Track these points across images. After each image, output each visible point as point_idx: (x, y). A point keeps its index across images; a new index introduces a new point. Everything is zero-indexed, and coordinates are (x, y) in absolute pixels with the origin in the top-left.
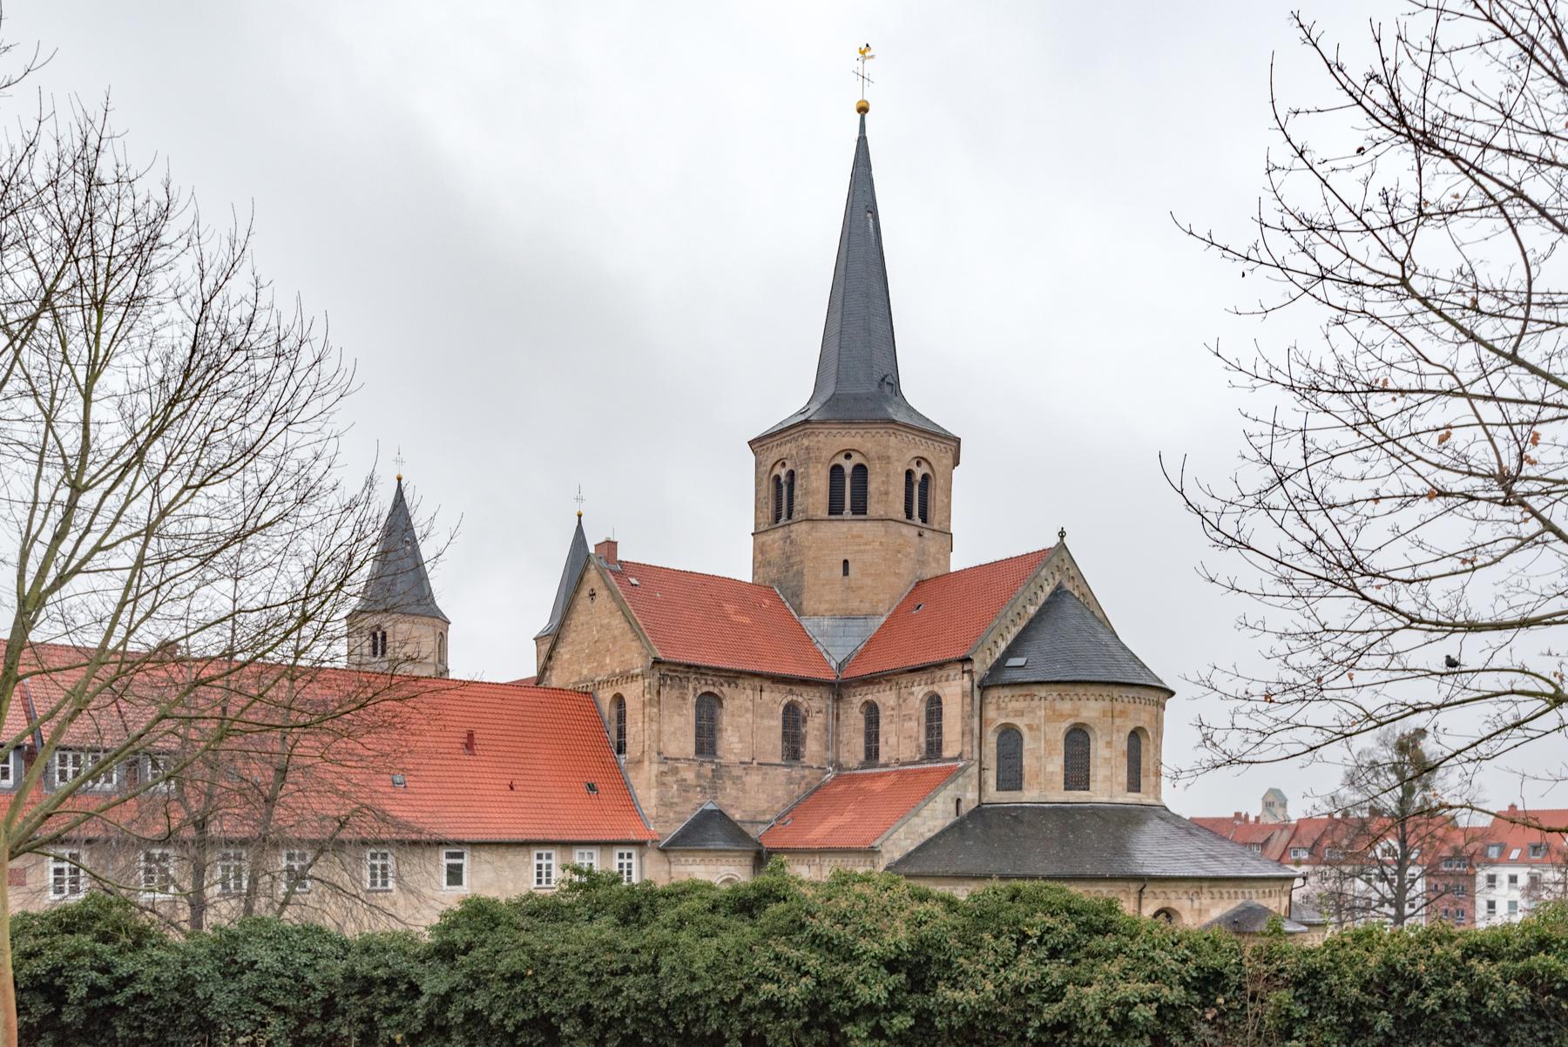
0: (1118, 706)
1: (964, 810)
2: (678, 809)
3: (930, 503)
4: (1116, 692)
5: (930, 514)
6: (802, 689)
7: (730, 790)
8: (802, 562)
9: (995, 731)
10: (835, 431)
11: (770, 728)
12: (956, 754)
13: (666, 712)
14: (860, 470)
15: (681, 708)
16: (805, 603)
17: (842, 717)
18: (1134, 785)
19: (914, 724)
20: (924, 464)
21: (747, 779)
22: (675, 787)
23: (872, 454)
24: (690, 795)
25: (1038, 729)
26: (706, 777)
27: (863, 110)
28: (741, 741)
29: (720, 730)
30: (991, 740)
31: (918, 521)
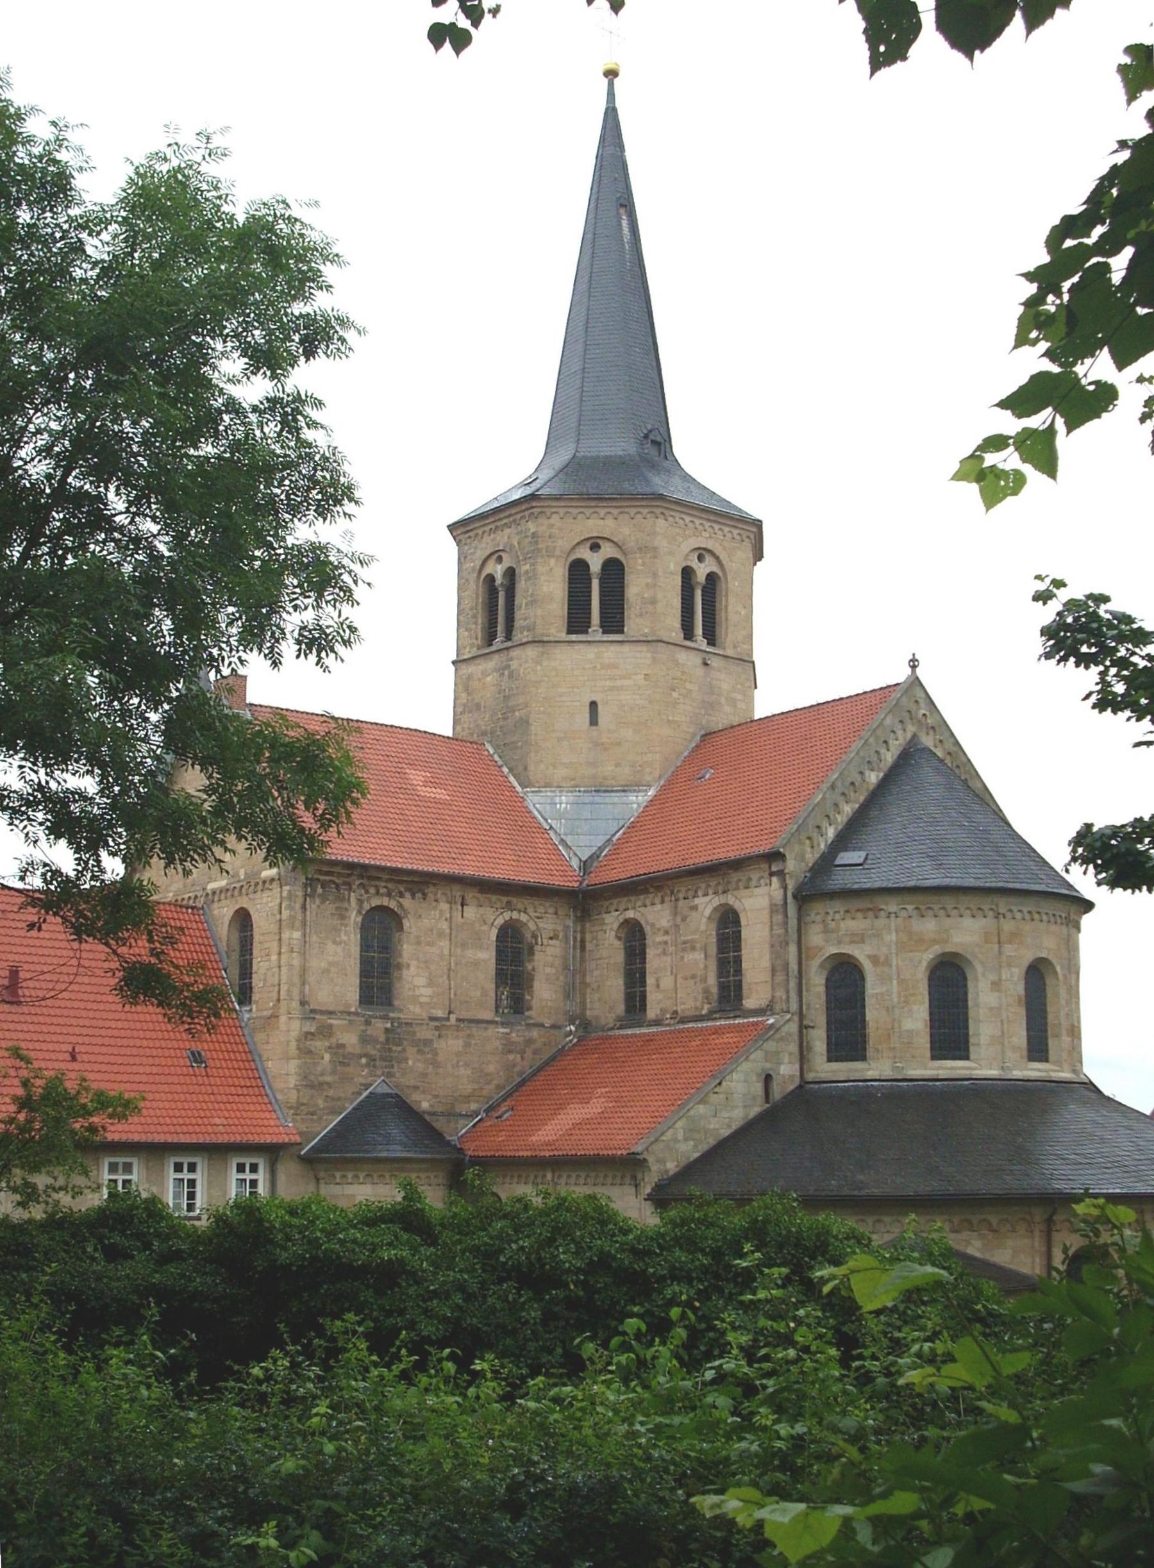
0: (1008, 926)
1: (777, 1093)
2: (331, 1093)
3: (721, 616)
4: (1003, 904)
5: (721, 631)
6: (525, 902)
7: (414, 1061)
8: (526, 705)
9: (822, 966)
10: (574, 511)
11: (476, 964)
12: (763, 1003)
13: (314, 938)
14: (614, 571)
15: (336, 930)
16: (531, 767)
17: (589, 946)
18: (1038, 1049)
19: (699, 956)
20: (708, 559)
21: (442, 1045)
22: (327, 1057)
23: (631, 544)
24: (350, 1069)
25: (887, 962)
26: (376, 1041)
27: (611, 74)
28: (431, 983)
29: (399, 967)
30: (817, 982)
31: (701, 642)
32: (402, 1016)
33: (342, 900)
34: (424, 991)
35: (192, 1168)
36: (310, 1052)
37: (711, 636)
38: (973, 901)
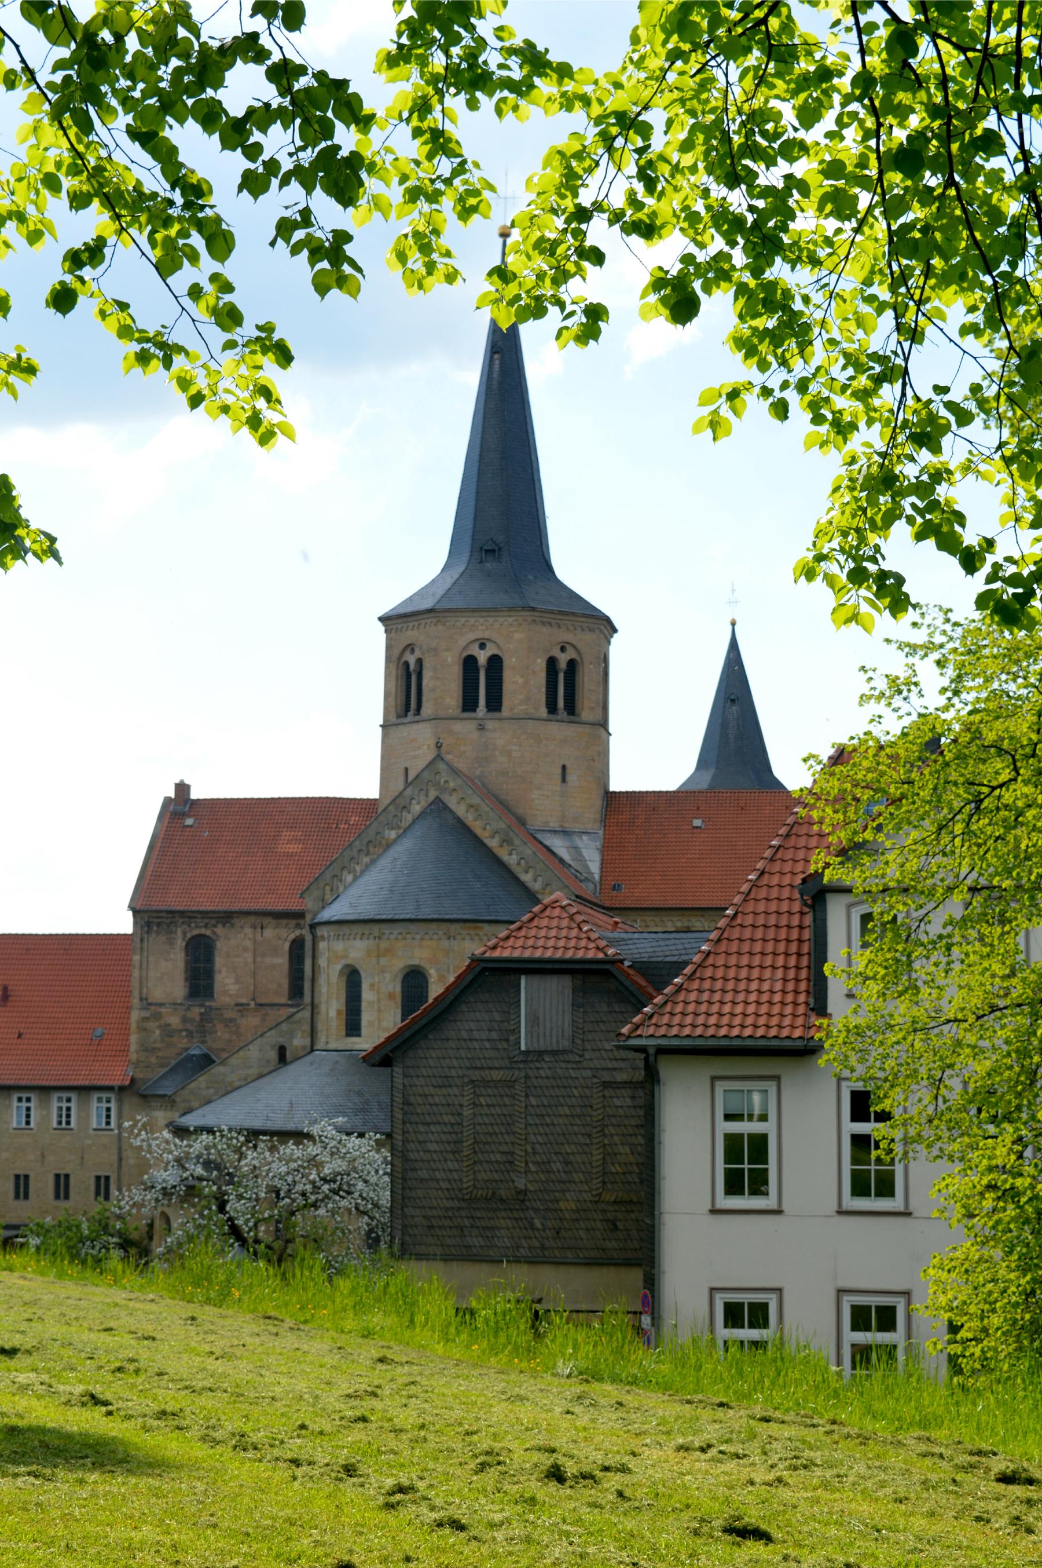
0: (384, 944)
2: (160, 1054)
4: (376, 929)
22: (158, 1032)
28: (237, 981)
32: (213, 1004)
33: (171, 932)
34: (231, 987)
35: (28, 1100)
36: (145, 1029)
37: (495, 703)
38: (357, 929)
